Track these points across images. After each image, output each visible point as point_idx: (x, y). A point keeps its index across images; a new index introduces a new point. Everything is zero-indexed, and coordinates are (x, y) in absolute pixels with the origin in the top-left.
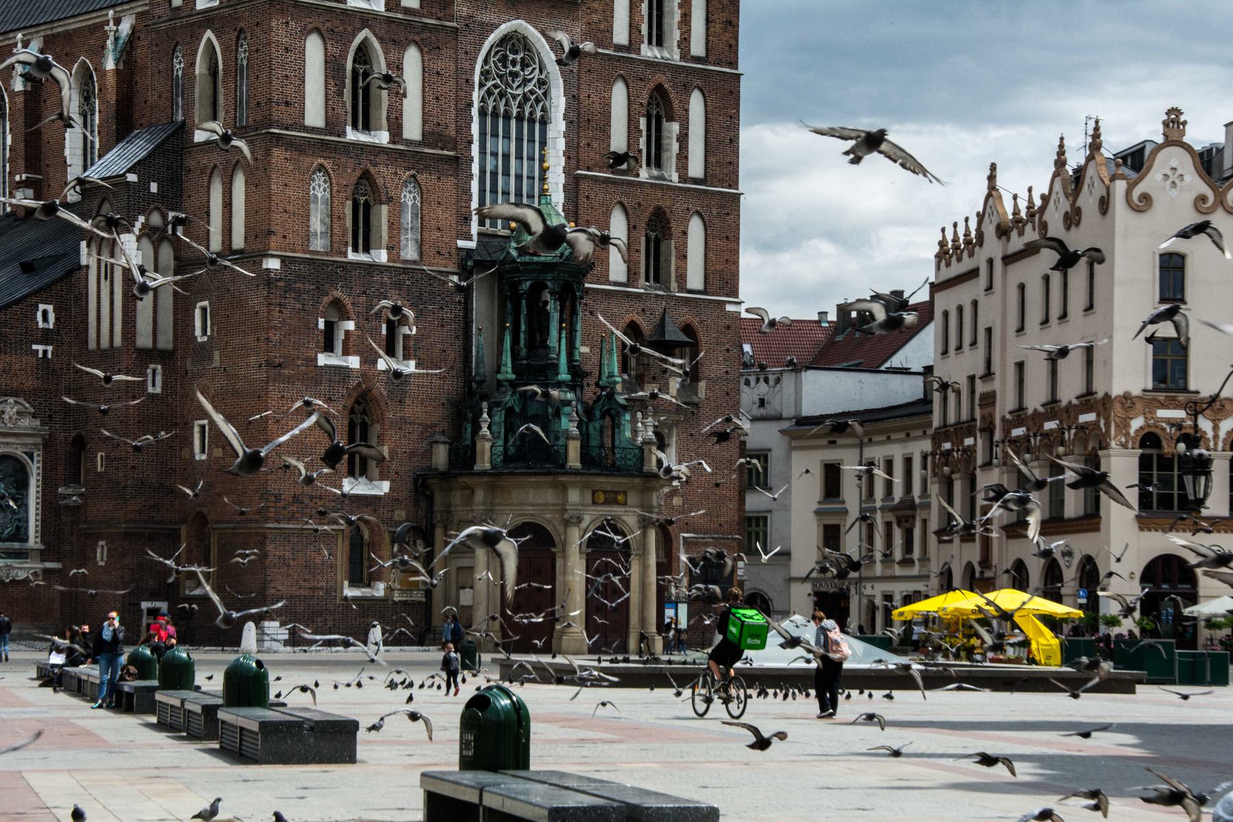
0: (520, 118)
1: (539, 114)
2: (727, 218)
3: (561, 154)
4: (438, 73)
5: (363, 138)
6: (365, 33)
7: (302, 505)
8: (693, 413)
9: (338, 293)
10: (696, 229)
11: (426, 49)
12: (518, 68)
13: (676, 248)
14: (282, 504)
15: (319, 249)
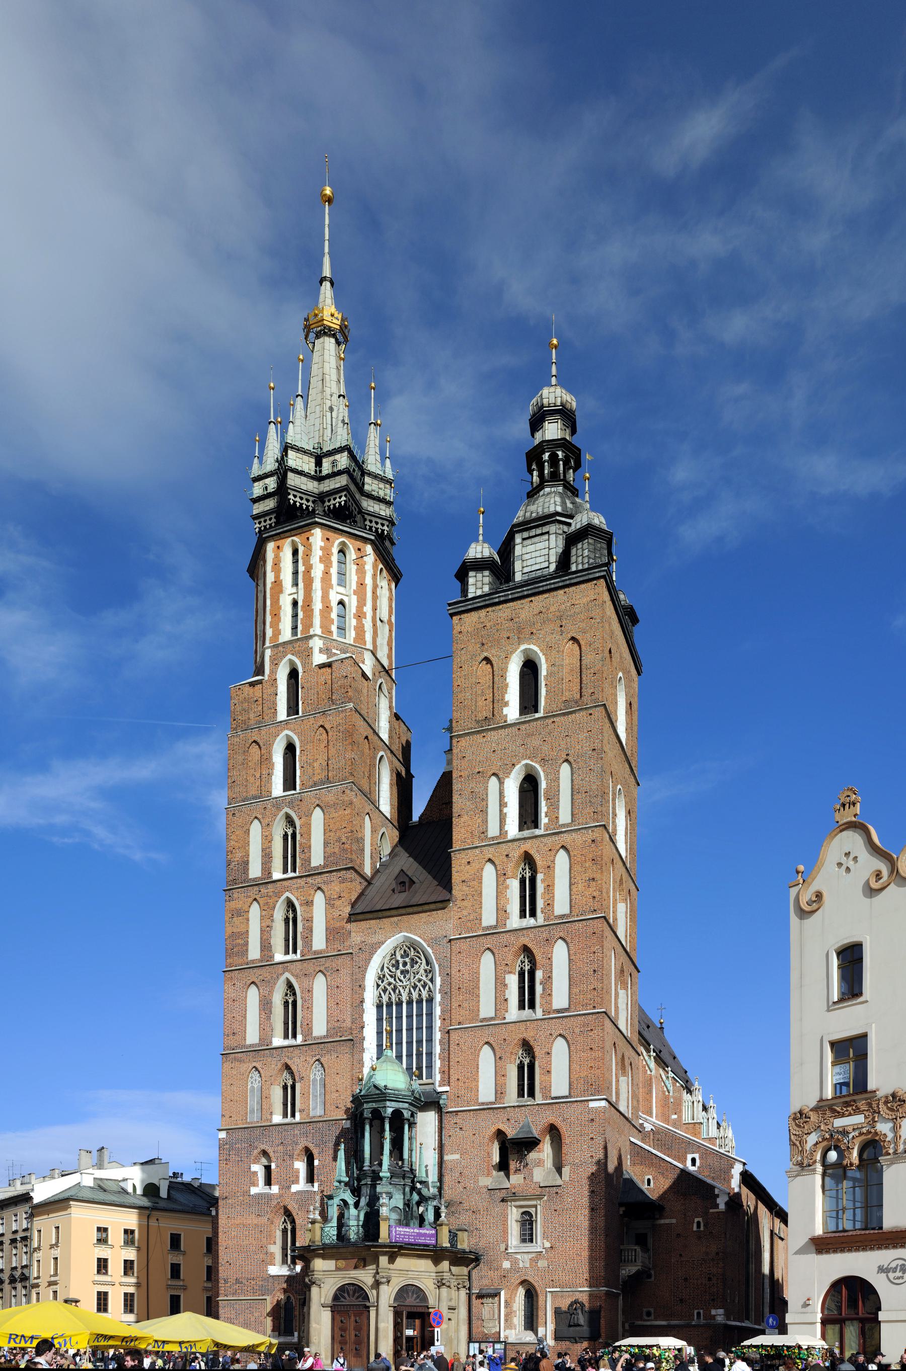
0: (410, 1003)
1: (425, 994)
2: (590, 1034)
3: (438, 1018)
4: (338, 987)
5: (286, 1043)
6: (287, 975)
7: (240, 1285)
8: (557, 1193)
9: (263, 1147)
10: (560, 1048)
11: (328, 974)
12: (408, 967)
13: (540, 1067)
14: (229, 1285)
15: (255, 1120)
